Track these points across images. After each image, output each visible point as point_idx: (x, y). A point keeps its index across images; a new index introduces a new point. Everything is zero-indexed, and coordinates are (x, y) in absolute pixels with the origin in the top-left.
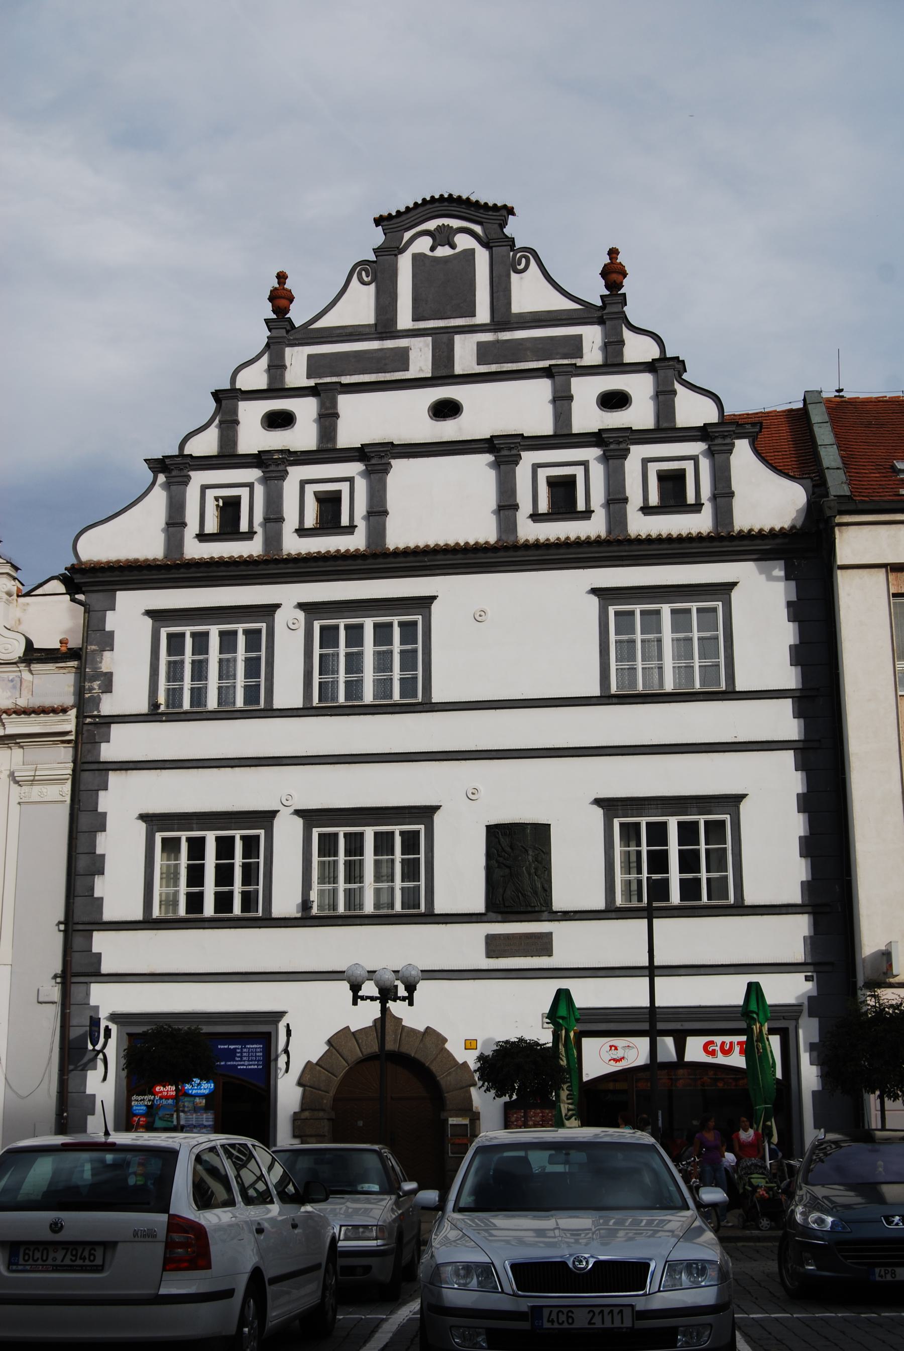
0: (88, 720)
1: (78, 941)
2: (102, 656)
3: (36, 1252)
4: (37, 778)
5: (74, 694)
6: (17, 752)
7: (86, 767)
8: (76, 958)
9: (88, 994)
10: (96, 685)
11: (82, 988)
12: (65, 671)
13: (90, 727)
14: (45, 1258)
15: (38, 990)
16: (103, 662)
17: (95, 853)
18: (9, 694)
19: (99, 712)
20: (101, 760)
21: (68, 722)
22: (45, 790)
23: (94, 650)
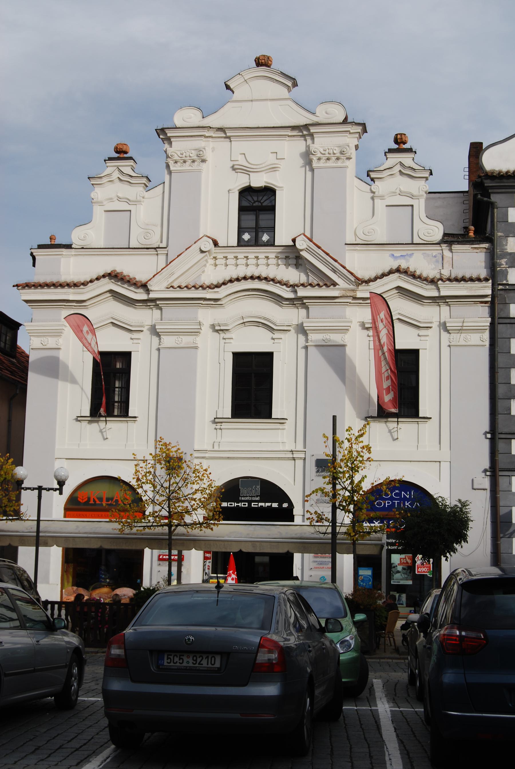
0: (500, 287)
1: (501, 446)
2: (507, 240)
3: (175, 657)
4: (464, 328)
5: (485, 268)
6: (445, 309)
7: (501, 321)
8: (501, 459)
9: (510, 483)
10: (503, 261)
11: (506, 479)
12: (477, 251)
13: (501, 292)
14: (213, 663)
15: (473, 480)
16: (508, 244)
17: (510, 383)
18: (433, 266)
19: (508, 281)
20: (511, 317)
21: (486, 289)
22: (469, 337)
23: (500, 236)
